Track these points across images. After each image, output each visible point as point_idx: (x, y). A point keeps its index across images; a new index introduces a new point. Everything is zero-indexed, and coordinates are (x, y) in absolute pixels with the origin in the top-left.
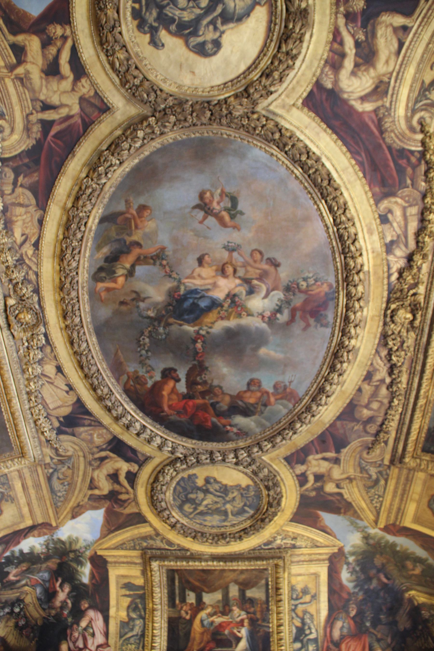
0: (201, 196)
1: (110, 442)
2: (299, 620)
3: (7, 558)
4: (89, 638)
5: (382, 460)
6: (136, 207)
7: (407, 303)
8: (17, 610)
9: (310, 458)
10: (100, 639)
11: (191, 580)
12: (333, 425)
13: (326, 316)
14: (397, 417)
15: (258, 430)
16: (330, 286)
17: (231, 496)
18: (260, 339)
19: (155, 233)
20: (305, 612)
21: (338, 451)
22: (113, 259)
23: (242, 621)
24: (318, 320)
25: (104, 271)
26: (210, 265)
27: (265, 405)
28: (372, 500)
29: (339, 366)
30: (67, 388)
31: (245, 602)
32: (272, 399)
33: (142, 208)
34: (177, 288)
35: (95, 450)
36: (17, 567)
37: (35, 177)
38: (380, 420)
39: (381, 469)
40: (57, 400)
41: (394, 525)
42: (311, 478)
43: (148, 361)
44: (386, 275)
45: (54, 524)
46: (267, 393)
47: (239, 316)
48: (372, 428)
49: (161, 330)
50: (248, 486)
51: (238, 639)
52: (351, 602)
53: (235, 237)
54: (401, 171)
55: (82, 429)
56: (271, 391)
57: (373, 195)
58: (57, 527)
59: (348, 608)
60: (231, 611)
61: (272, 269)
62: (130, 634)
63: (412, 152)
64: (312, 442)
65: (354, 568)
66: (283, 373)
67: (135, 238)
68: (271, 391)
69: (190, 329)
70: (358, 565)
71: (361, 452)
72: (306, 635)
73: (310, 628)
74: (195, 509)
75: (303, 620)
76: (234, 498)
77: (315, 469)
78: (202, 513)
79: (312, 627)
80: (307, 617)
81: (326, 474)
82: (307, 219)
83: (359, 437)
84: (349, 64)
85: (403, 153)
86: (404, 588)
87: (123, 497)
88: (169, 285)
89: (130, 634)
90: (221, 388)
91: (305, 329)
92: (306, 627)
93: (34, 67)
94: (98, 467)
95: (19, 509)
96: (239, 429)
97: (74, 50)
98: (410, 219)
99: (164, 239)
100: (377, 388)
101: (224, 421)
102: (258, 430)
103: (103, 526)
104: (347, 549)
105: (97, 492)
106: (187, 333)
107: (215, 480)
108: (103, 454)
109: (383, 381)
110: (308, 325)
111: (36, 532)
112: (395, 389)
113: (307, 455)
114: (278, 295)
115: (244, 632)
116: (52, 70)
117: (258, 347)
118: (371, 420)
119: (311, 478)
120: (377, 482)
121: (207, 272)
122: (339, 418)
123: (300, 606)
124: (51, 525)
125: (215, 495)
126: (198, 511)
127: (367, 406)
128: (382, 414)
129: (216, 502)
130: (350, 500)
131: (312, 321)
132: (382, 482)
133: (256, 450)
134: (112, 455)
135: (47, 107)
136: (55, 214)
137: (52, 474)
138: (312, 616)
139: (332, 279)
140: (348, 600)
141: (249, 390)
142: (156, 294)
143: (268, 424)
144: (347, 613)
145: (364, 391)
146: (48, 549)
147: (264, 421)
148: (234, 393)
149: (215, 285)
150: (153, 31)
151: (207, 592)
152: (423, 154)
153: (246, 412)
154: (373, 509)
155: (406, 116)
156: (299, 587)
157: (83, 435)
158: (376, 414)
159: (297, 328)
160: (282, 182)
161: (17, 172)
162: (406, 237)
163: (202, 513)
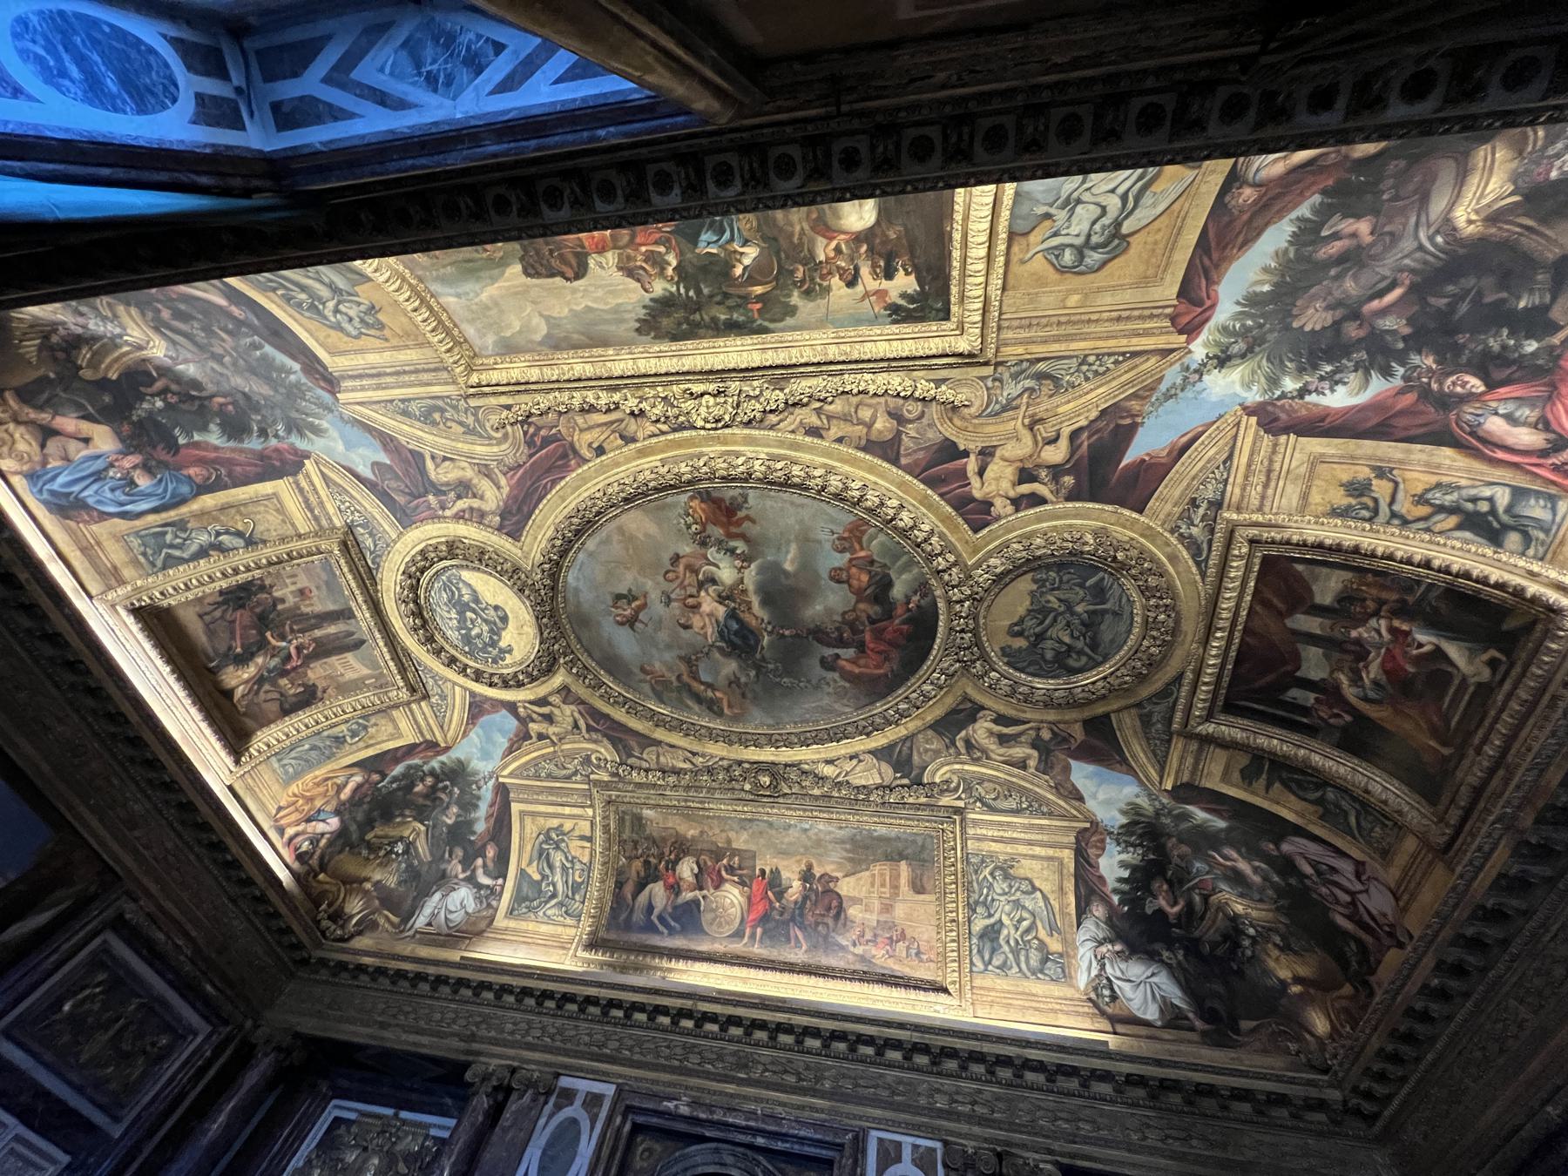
0: (622, 624)
1: (940, 734)
2: (1441, 516)
3: (1122, 902)
4: (1336, 878)
5: (982, 378)
6: (642, 676)
7: (690, 404)
8: (1251, 931)
9: (977, 494)
10: (1346, 867)
11: (1258, 684)
12: (908, 469)
13: (733, 498)
14: (881, 378)
15: (916, 570)
16: (692, 498)
17: (1055, 604)
18: (772, 573)
19: (665, 663)
20: (1421, 500)
21: (966, 454)
22: (699, 699)
23: (1391, 630)
24: (740, 507)
25: (713, 707)
26: (689, 619)
27: (872, 562)
28: (1096, 373)
29: (796, 480)
30: (855, 762)
31: (1347, 608)
32: (862, 554)
33: (643, 670)
34: (720, 649)
35: (952, 751)
36: (1155, 897)
37: (633, 743)
38: (892, 402)
39: (1006, 376)
40: (870, 774)
41: (1173, 319)
42: (1025, 488)
43: (814, 682)
44: (662, 438)
45: (1088, 825)
46: (851, 560)
47: (744, 592)
48: (913, 409)
49: (771, 666)
50: (1035, 581)
51: (1438, 653)
52: (1435, 386)
53: (655, 596)
54: (546, 441)
55: (915, 757)
56: (848, 555)
57: (579, 466)
58: (1095, 824)
59: (1452, 395)
60: (1358, 642)
61: (683, 562)
62: (1353, 820)
63: (525, 433)
64: (941, 495)
65: (1322, 379)
66: (819, 542)
67: (673, 678)
68: (848, 555)
69: (766, 640)
70: (1315, 367)
71: (963, 418)
72: (1493, 511)
73: (1474, 500)
74: (1080, 653)
75: (1441, 509)
76: (1060, 600)
77: (1005, 485)
78: (1094, 646)
79: (1473, 492)
80: (1438, 497)
81: (1019, 464)
82: (621, 530)
83: (931, 425)
84: (476, 503)
85: (530, 443)
86: (1439, 239)
87: (1046, 735)
88: (717, 655)
89: (1353, 820)
90: (844, 613)
91: (754, 522)
92: (1470, 506)
93: (552, 730)
94: (984, 751)
95: (1033, 857)
96: (915, 593)
97: (531, 702)
98: (591, 423)
99: (668, 656)
100: (829, 418)
101: (900, 611)
102: (916, 570)
103: (1109, 766)
104: (1254, 396)
105: (1032, 763)
106: (771, 644)
107: (1015, 625)
108: (960, 744)
109: (818, 411)
110: (748, 518)
111: (1092, 852)
112: (824, 395)
113: (973, 500)
114: (712, 553)
115: (1425, 639)
116: (549, 718)
117: (786, 573)
118: (897, 417)
119: (1025, 488)
120: (1041, 377)
121: (697, 622)
122: (895, 461)
123: (1395, 508)
124: (1086, 829)
125: (1051, 625)
126: (1087, 650)
127: (869, 426)
128: (882, 400)
129: (1068, 625)
130: (1094, 414)
131: (741, 514)
132: (1041, 366)
133: (946, 577)
134: (963, 733)
135: (576, 726)
136: (659, 734)
137: (984, 804)
138: (1438, 485)
139: (684, 498)
140: (1425, 393)
141: (847, 582)
142: (730, 667)
143: (904, 559)
144: (1470, 397)
145: (840, 434)
146: (1141, 845)
147: (899, 563)
148: (853, 598)
149: (710, 615)
150: (502, 651)
151: (1299, 668)
152: (522, 423)
153: (889, 584)
154: (1125, 366)
155: (499, 444)
156: (1340, 499)
157: (926, 758)
158: (881, 409)
159: (753, 530)
160: (591, 554)
161: (630, 755)
162: (612, 423)
163: (1094, 646)
